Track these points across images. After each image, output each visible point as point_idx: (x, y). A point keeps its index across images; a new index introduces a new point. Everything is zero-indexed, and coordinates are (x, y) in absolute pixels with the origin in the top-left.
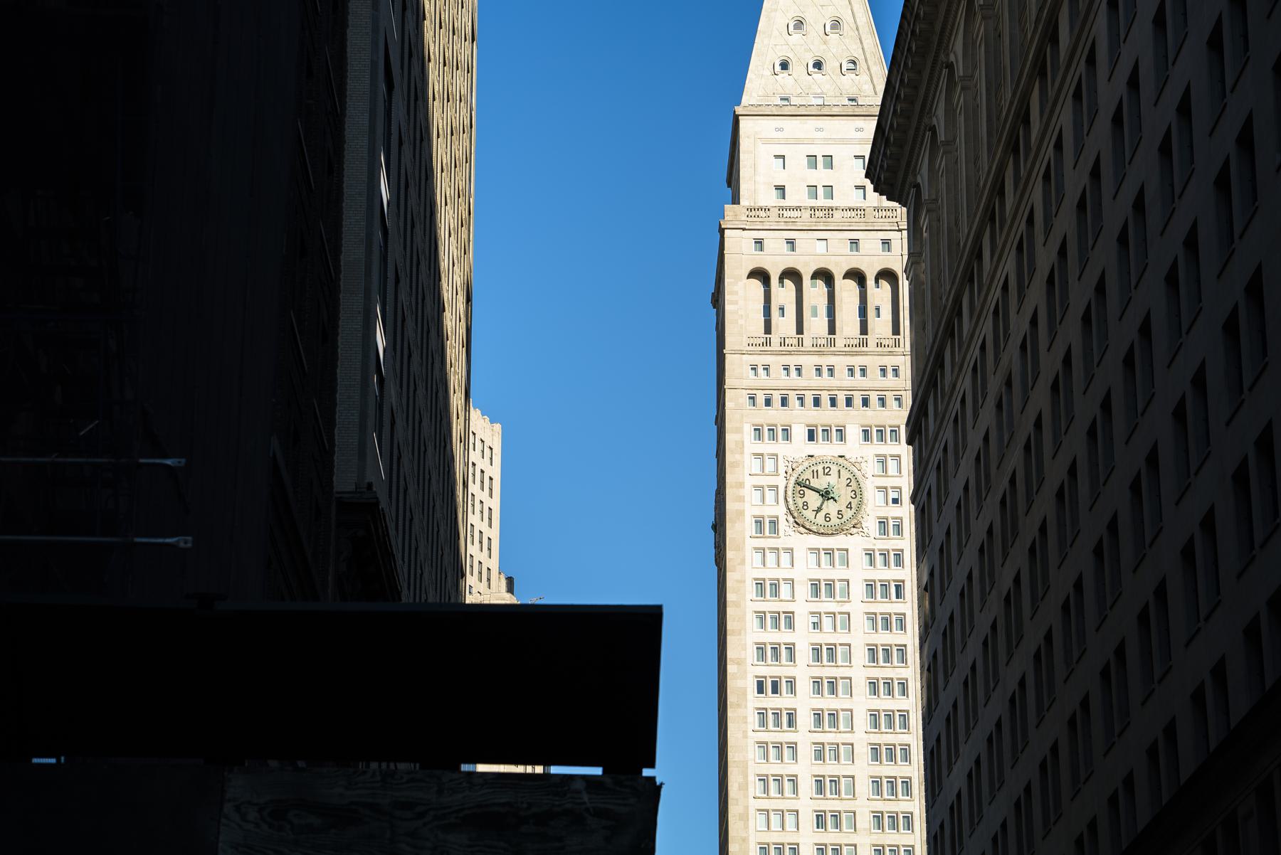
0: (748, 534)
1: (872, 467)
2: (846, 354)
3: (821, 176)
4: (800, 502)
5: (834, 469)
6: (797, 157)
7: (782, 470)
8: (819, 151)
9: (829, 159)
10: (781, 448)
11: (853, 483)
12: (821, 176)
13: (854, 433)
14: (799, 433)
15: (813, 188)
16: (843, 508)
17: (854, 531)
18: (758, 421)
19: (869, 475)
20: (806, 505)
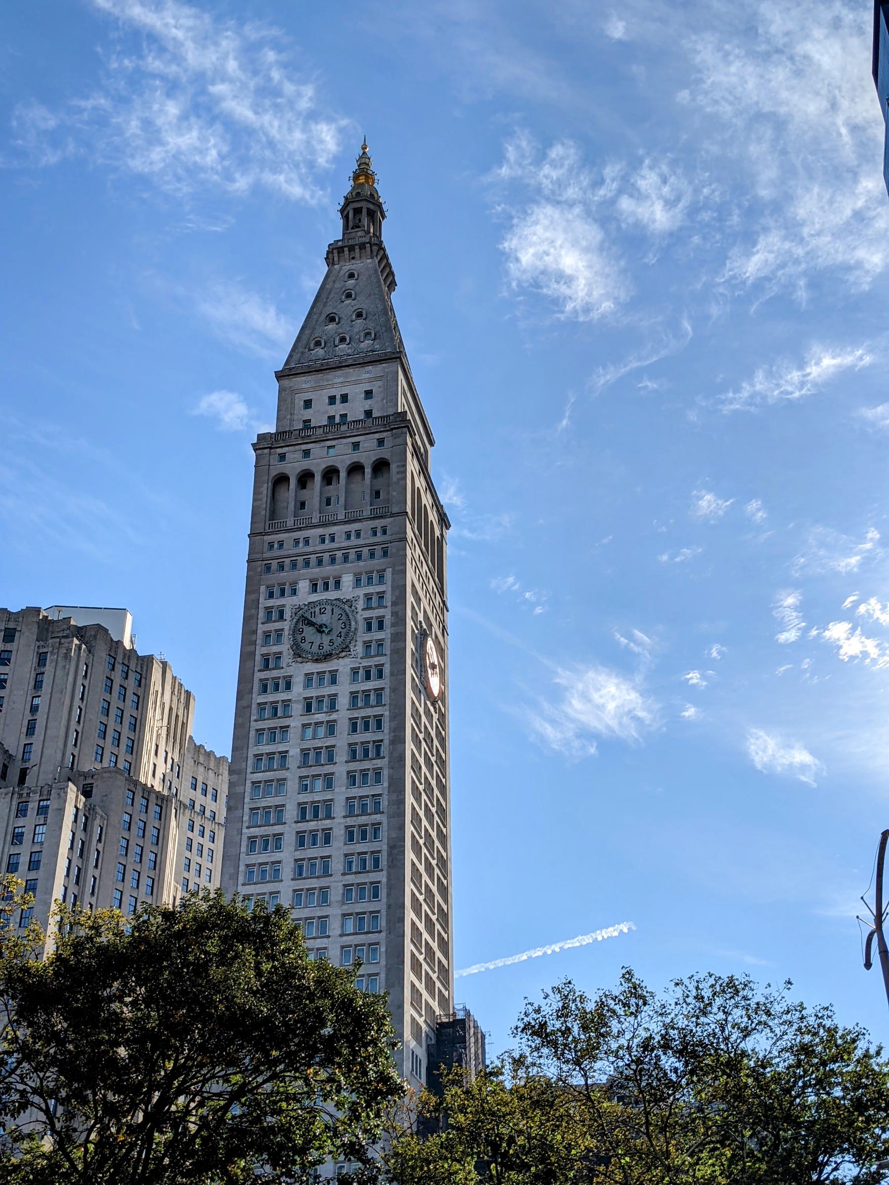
0: (256, 669)
1: (361, 604)
2: (346, 523)
3: (338, 409)
4: (299, 637)
5: (329, 608)
6: (320, 399)
7: (287, 615)
8: (337, 393)
9: (344, 398)
10: (289, 603)
11: (344, 618)
12: (338, 409)
13: (347, 580)
14: (303, 586)
15: (331, 418)
16: (334, 637)
17: (343, 654)
18: (270, 583)
19: (359, 609)
20: (304, 639)
